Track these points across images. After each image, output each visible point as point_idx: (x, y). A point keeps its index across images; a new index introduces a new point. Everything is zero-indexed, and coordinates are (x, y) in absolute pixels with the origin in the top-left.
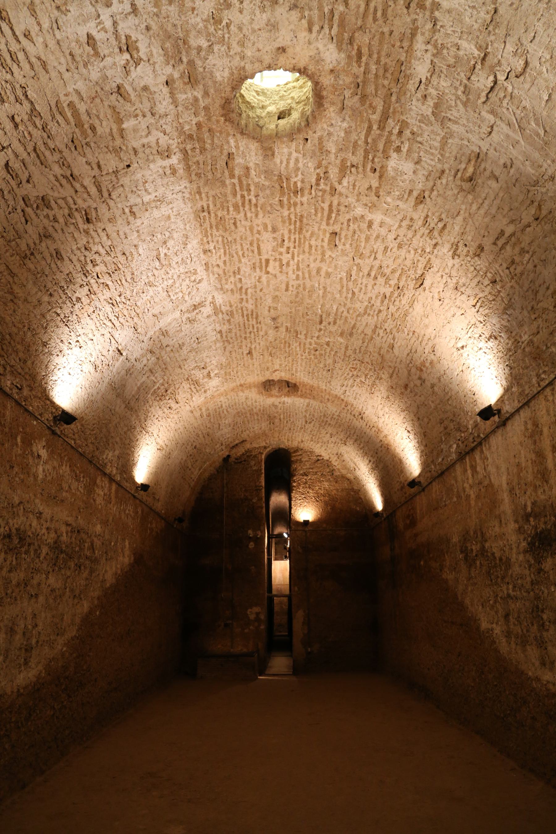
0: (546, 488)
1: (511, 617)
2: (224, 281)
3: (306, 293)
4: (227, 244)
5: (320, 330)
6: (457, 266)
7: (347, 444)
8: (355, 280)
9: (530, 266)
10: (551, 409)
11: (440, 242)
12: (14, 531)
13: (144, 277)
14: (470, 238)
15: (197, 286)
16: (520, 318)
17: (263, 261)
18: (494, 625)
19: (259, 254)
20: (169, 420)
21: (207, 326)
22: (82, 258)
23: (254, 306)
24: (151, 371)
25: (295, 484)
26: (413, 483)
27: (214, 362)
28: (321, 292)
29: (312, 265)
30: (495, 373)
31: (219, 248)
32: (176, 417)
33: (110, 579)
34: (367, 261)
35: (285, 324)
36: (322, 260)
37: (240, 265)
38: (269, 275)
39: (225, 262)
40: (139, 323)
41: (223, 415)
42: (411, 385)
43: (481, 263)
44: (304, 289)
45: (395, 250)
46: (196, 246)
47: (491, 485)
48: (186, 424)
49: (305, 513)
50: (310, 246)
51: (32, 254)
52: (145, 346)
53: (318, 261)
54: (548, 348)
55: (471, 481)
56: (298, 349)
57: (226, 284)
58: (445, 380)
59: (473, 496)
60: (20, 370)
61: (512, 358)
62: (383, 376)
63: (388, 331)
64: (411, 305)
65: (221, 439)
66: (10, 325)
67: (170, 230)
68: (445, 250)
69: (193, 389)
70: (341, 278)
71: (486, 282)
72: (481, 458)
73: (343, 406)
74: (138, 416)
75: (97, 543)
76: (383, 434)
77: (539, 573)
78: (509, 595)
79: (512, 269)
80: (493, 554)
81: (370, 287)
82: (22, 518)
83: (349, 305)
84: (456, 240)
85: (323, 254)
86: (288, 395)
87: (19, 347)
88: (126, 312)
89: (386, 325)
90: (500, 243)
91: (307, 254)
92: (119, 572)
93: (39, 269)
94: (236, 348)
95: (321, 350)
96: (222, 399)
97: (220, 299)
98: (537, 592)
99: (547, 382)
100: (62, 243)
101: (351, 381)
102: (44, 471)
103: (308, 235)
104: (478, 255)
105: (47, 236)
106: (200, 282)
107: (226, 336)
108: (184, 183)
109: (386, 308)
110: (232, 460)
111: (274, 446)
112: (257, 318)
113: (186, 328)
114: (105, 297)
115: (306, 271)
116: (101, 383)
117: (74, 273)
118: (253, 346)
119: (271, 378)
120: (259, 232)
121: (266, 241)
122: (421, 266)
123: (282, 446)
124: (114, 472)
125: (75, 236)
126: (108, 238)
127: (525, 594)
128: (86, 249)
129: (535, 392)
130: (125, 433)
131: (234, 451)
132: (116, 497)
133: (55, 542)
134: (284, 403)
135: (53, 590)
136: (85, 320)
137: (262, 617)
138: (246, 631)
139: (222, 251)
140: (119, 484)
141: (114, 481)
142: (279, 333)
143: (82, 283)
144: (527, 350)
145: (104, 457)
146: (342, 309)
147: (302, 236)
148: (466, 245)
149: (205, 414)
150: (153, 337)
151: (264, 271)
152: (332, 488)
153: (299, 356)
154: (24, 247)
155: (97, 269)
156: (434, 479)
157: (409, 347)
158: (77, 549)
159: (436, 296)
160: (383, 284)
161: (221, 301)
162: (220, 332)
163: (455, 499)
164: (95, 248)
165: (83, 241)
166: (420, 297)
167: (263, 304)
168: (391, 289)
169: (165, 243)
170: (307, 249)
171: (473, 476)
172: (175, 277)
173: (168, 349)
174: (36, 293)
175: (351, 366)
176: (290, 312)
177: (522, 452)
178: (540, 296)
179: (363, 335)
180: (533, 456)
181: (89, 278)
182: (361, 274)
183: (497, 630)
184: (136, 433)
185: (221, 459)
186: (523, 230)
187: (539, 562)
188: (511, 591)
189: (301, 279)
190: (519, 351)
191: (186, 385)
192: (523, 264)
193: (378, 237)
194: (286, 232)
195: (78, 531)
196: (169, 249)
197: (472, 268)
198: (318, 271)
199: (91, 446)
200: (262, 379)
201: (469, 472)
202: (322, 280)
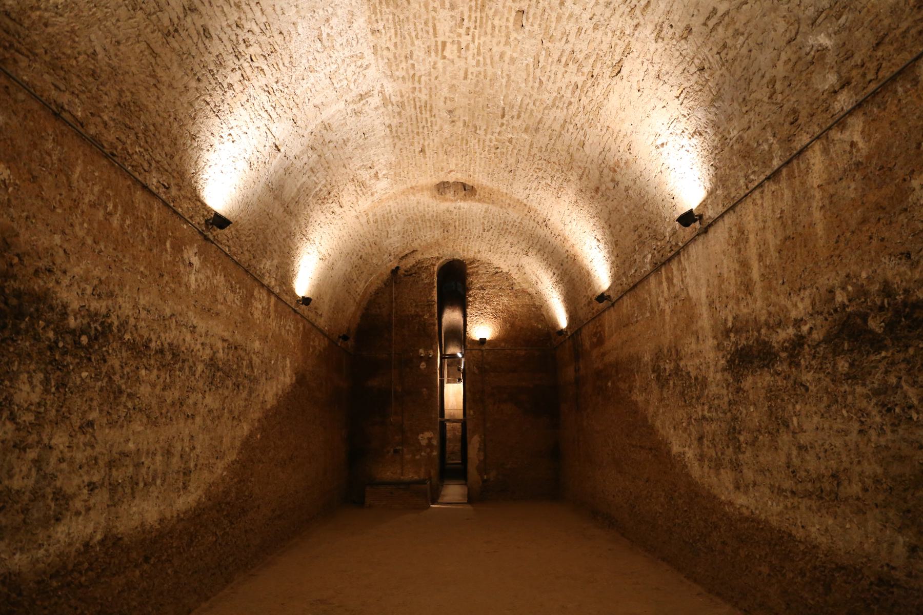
0: (750, 301)
1: (705, 440)
2: (394, 68)
3: (487, 82)
4: (398, 23)
5: (502, 124)
6: (660, 50)
7: (529, 254)
8: (543, 67)
9: (744, 51)
10: (760, 213)
11: (642, 22)
12: (166, 346)
13: (304, 61)
14: (676, 18)
15: (364, 72)
16: (729, 111)
17: (439, 43)
18: (687, 449)
19: (435, 35)
20: (332, 226)
21: (375, 119)
22: (234, 37)
23: (427, 98)
24: (312, 170)
25: (470, 299)
26: (602, 298)
28: (504, 81)
29: (494, 50)
30: (699, 174)
31: (389, 28)
32: (340, 222)
33: (271, 400)
34: (558, 44)
35: (462, 118)
36: (507, 43)
37: (413, 48)
38: (446, 61)
39: (395, 44)
40: (298, 114)
41: (391, 222)
42: (603, 188)
43: (688, 47)
44: (485, 77)
45: (589, 32)
46: (364, 25)
47: (688, 298)
48: (351, 231)
49: (482, 329)
50: (494, 27)
51: (176, 30)
52: (306, 141)
53: (502, 44)
54: (759, 145)
55: (666, 294)
56: (477, 147)
57: (397, 70)
58: (641, 182)
59: (668, 311)
60: (166, 167)
61: (718, 157)
62: (572, 178)
63: (579, 126)
64: (606, 97)
65: (389, 248)
66: (154, 114)
67: (333, 5)
68: (647, 31)
70: (527, 65)
71: (693, 69)
72: (678, 270)
73: (526, 212)
74: (298, 221)
75: (256, 360)
76: (570, 243)
77: (738, 392)
78: (704, 417)
79: (723, 55)
80: (688, 373)
81: (560, 76)
82: (174, 332)
83: (535, 96)
84: (661, 20)
85: (508, 36)
86: (464, 199)
87: (164, 139)
88: (283, 102)
90: (711, 23)
91: (489, 36)
92: (280, 393)
93: (185, 49)
94: (407, 145)
96: (391, 203)
97: (390, 88)
98: (735, 412)
99: (756, 184)
100: (210, 19)
101: (536, 183)
102: (196, 280)
103: (491, 13)
104: (686, 38)
105: (193, 10)
106: (367, 67)
109: (577, 99)
110: (401, 272)
111: (448, 257)
112: (431, 111)
113: (351, 121)
114: (260, 84)
115: (488, 55)
116: (257, 182)
117: (224, 54)
118: (426, 143)
119: (445, 180)
120: (435, 10)
121: (442, 20)
122: (619, 50)
123: (457, 257)
124: (273, 283)
125: (225, 10)
126: (263, 13)
127: (721, 415)
128: (237, 26)
129: (743, 195)
130: (284, 240)
131: (404, 261)
132: (276, 311)
133: (211, 359)
134: (459, 208)
135: (210, 411)
136: (238, 110)
137: (435, 442)
138: (418, 457)
139: (393, 31)
140: (278, 297)
141: (273, 293)
143: (234, 66)
144: (735, 147)
145: (262, 266)
146: (527, 100)
147: (484, 15)
148: (671, 26)
149: (371, 220)
150: (315, 131)
151: (440, 56)
152: (512, 304)
153: (478, 154)
154: (166, 22)
155: (251, 50)
156: (625, 293)
157: (602, 145)
158: (235, 367)
159: (635, 86)
160: (575, 71)
162: (390, 126)
163: (648, 314)
164: (248, 26)
165: (234, 16)
166: (616, 87)
167: (438, 95)
168: (584, 78)
169: (327, 20)
170: (489, 30)
171: (669, 289)
172: (339, 61)
173: (332, 145)
174: (182, 77)
175: (535, 166)
176: (469, 104)
177: (725, 261)
178: (753, 86)
179: (550, 131)
180: (737, 266)
181: (242, 60)
182: (550, 60)
183: (690, 454)
184: (296, 240)
185: (389, 272)
186: (739, 8)
187: (738, 381)
188: (706, 413)
189: (481, 65)
190: (727, 149)
191: (351, 187)
192: (736, 48)
193: (571, 16)
194: (466, 10)
195: (236, 348)
196: (332, 28)
197: (678, 54)
198: (502, 56)
199: (247, 253)
200: (436, 181)
201: (665, 284)
202: (506, 66)
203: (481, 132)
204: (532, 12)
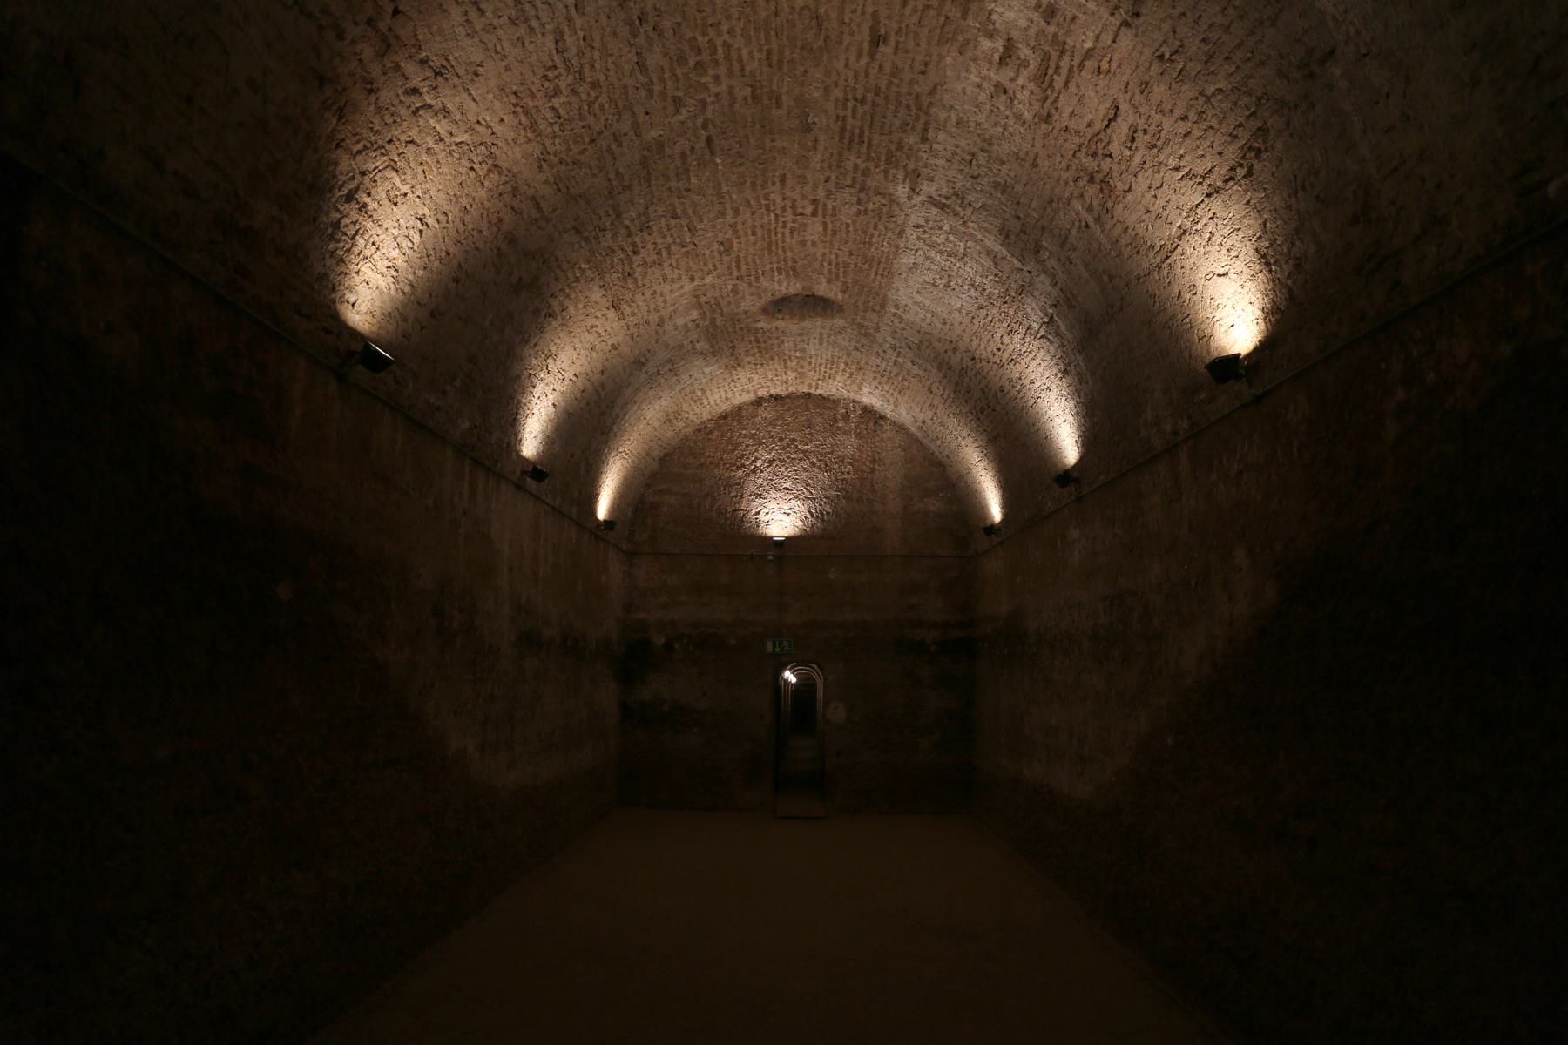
3: (749, 180)
27: (974, 78)
28: (725, 189)
44: (753, 183)
50: (754, 234)
56: (745, 52)
69: (1064, 72)
85: (735, 231)
94: (907, 76)
95: (686, 76)
97: (902, 191)
106: (917, 226)
107: (917, 119)
108: (892, 295)
112: (843, 129)
118: (863, 62)
161: (900, 188)
162: (924, 140)
170: (759, 232)
203: (743, 93)
204: (718, 258)
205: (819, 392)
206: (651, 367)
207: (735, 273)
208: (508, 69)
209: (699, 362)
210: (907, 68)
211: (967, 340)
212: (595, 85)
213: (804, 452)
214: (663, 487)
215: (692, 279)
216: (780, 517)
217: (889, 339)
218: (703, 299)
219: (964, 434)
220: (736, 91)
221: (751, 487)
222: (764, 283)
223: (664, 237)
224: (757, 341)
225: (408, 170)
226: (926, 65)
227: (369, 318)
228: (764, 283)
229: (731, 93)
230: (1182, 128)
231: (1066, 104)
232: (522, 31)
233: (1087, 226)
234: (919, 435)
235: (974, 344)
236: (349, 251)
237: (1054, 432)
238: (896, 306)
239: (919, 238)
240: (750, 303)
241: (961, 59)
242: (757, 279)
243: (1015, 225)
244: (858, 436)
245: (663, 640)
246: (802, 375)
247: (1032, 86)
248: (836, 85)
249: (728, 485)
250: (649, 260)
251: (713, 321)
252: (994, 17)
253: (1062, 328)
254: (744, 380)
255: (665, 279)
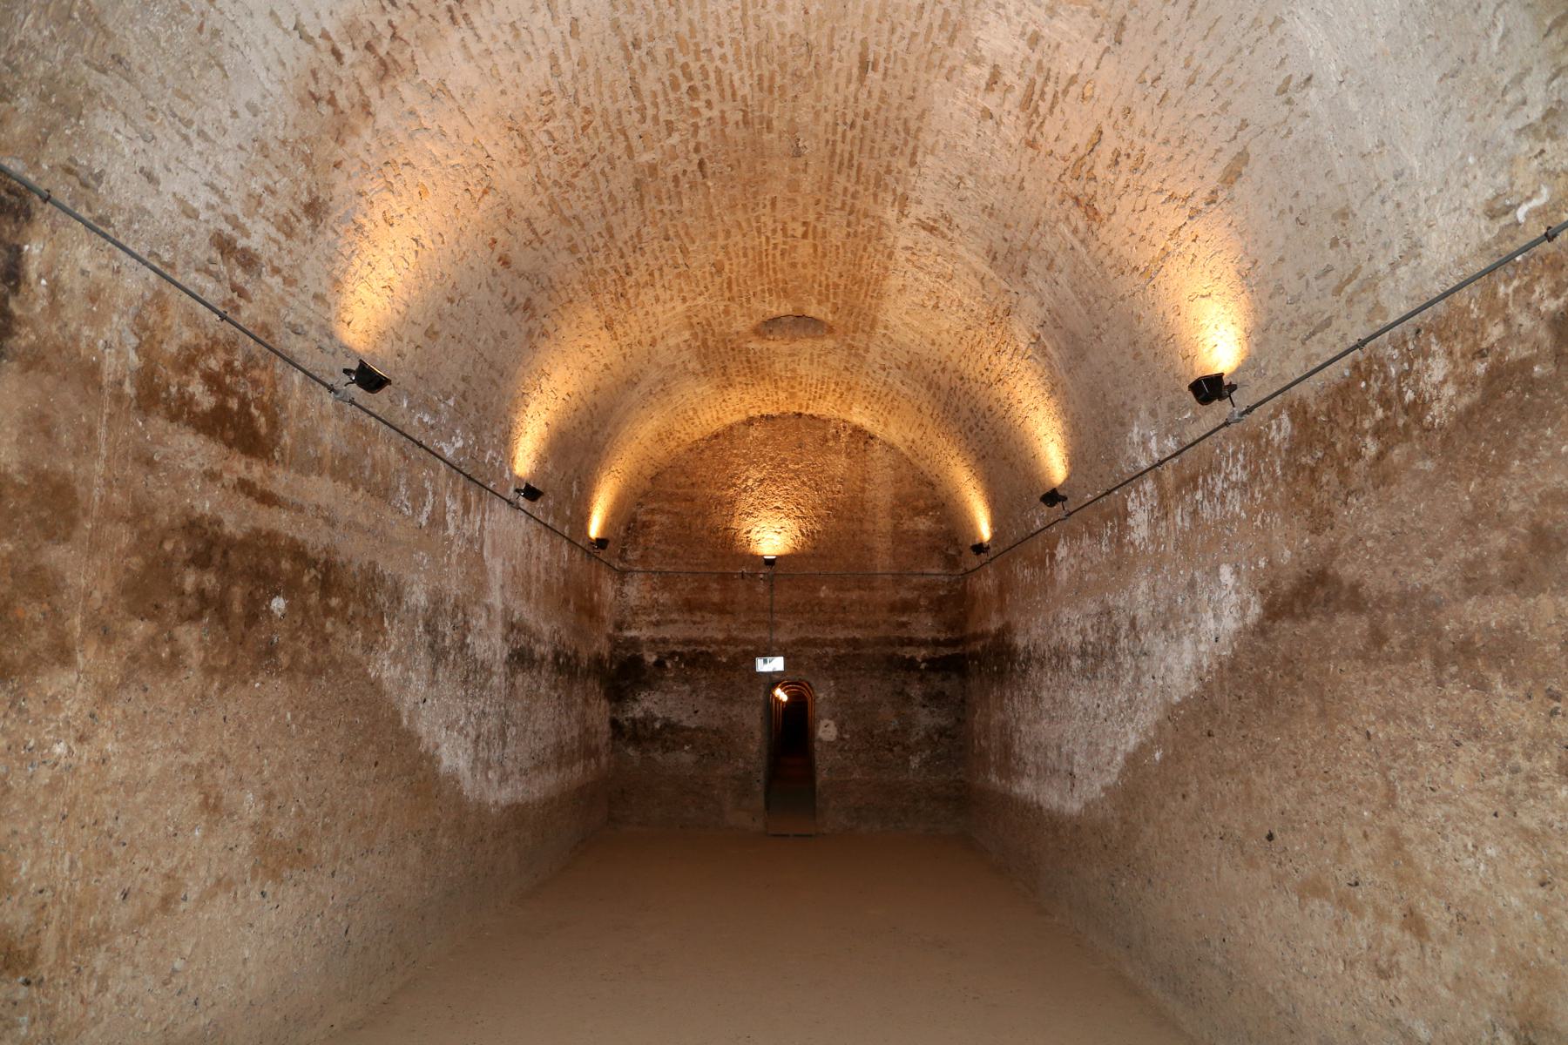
2: (875, 232)
23: (836, 177)
29: (739, 237)
36: (725, 247)
39: (865, 249)
56: (736, 78)
69: (1049, 97)
85: (727, 253)
89: (602, 258)
97: (891, 214)
106: (907, 248)
107: (906, 143)
108: (881, 317)
112: (833, 153)
118: (853, 87)
142: (787, 117)
161: (889, 210)
162: (913, 163)
170: (750, 253)
203: (735, 117)
205: (810, 412)
206: (643, 387)
207: (727, 295)
208: (503, 92)
209: (691, 381)
210: (895, 94)
211: (955, 360)
212: (587, 111)
213: (794, 471)
214: (655, 505)
215: (684, 300)
216: (771, 536)
217: (879, 359)
218: (695, 320)
219: (953, 453)
220: (727, 115)
221: (742, 506)
222: (755, 303)
223: (657, 258)
224: (748, 361)
225: (405, 193)
226: (914, 90)
227: (364, 337)
228: (755, 303)
229: (723, 118)
230: (1165, 152)
231: (1051, 128)
232: (518, 56)
233: (1072, 248)
234: (909, 454)
235: (963, 365)
236: (345, 271)
237: (1042, 451)
238: (886, 327)
239: (908, 260)
240: (741, 324)
241: (949, 85)
242: (748, 300)
243: (1002, 248)
244: (848, 455)
245: (654, 658)
246: (793, 395)
247: (1016, 111)
248: (826, 110)
249: (719, 502)
250: (642, 281)
251: (705, 342)
252: (980, 44)
253: (1050, 348)
254: (735, 400)
255: (657, 300)
